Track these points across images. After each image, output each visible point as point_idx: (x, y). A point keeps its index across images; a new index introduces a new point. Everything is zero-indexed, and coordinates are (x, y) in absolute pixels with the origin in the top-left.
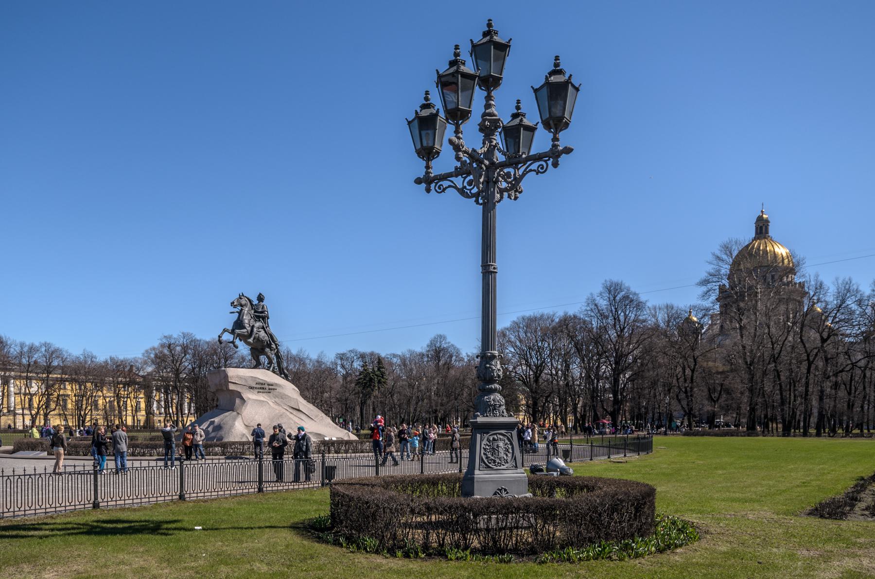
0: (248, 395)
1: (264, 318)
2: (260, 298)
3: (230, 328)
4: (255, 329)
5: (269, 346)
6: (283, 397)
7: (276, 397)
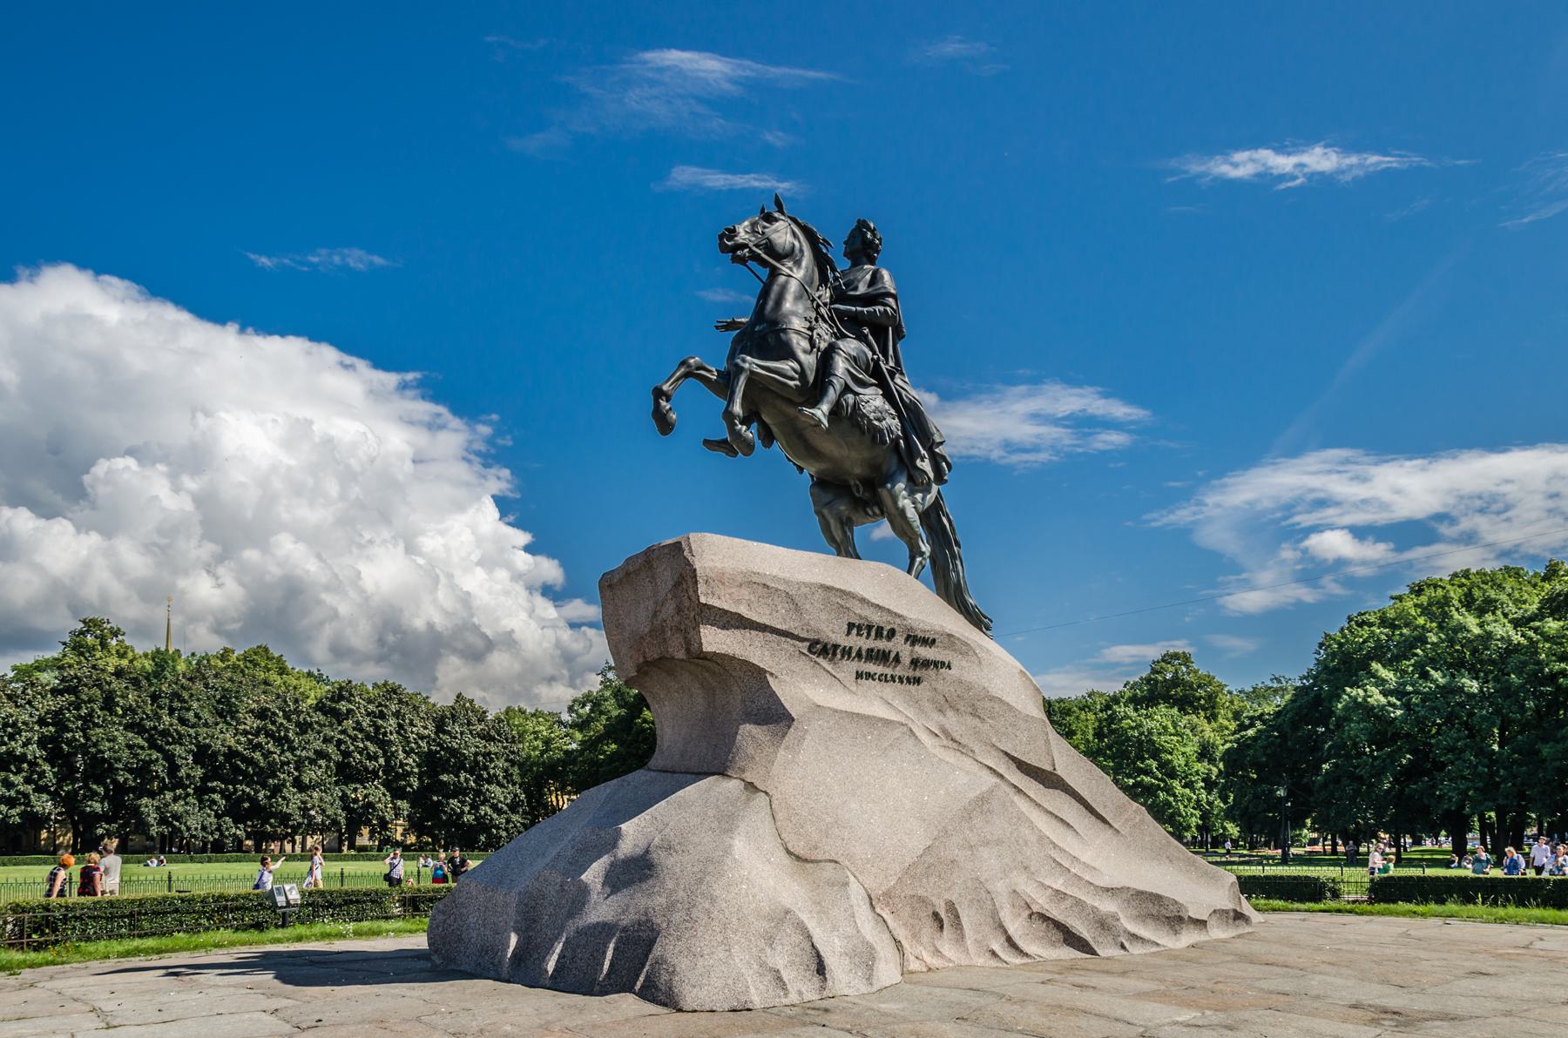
0: (801, 686)
1: (879, 332)
4: (841, 365)
5: (906, 460)
6: (976, 704)
7: (947, 704)
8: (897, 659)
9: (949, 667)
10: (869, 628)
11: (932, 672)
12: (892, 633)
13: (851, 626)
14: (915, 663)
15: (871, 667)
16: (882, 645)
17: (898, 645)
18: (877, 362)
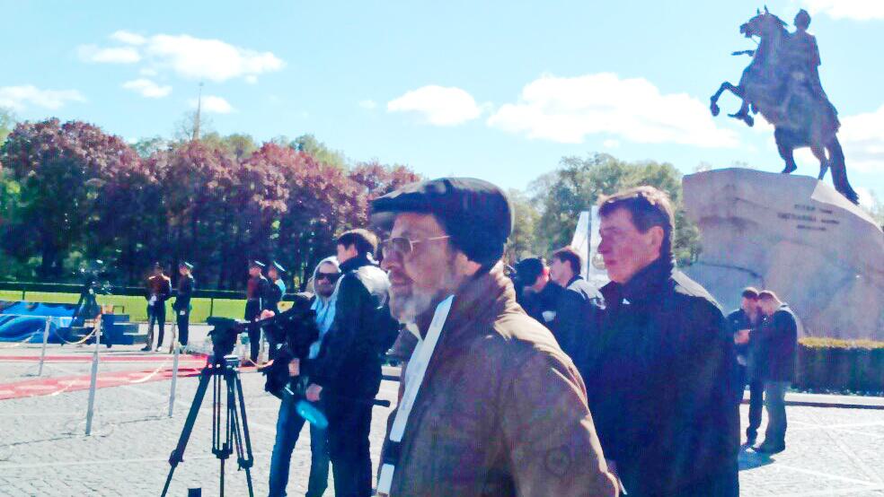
3: (736, 83)
8: (815, 220)
12: (813, 209)
14: (823, 221)
16: (807, 214)
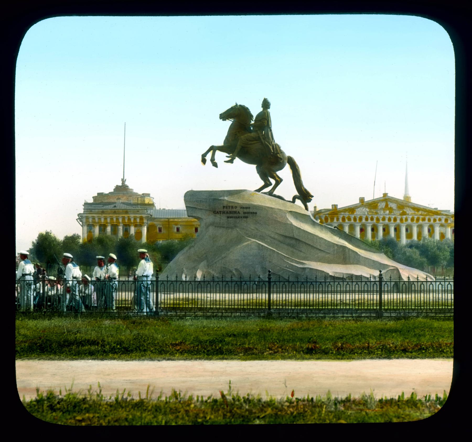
2: (266, 104)
8: (239, 212)
9: (256, 213)
10: (229, 206)
11: (251, 215)
13: (224, 207)
14: (244, 213)
15: (231, 215)
16: (234, 210)
17: (238, 209)
18: (259, 137)
